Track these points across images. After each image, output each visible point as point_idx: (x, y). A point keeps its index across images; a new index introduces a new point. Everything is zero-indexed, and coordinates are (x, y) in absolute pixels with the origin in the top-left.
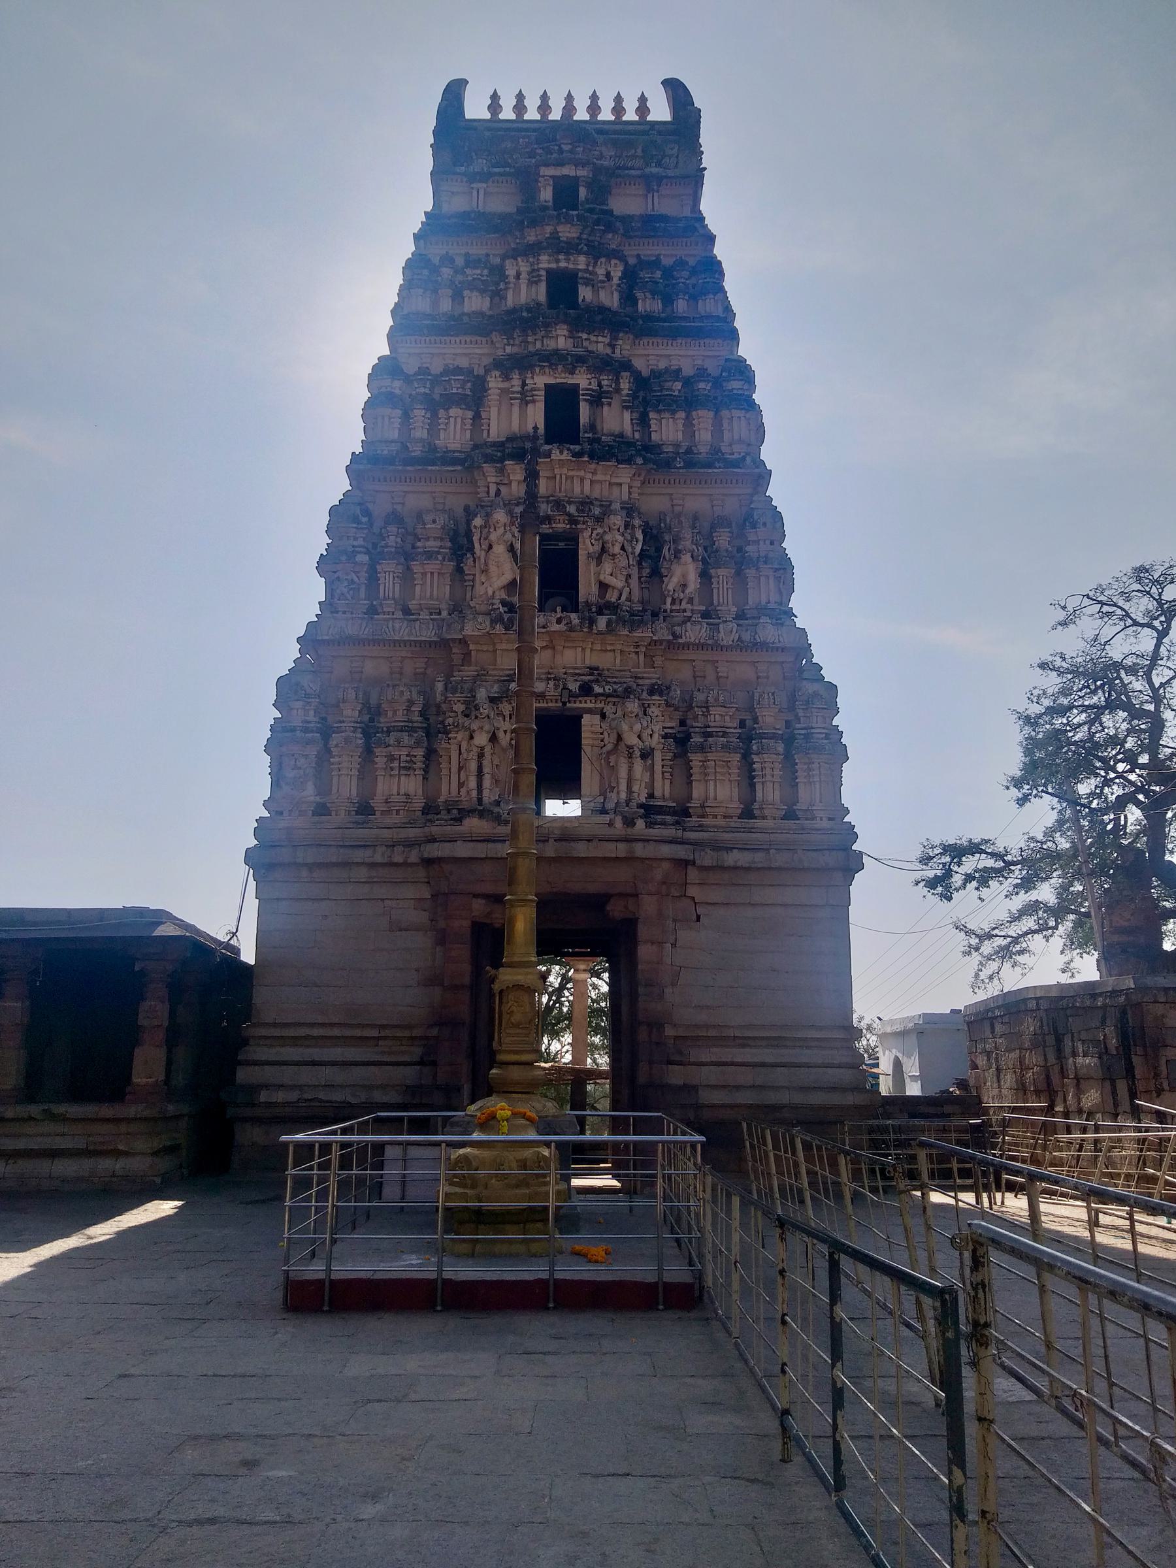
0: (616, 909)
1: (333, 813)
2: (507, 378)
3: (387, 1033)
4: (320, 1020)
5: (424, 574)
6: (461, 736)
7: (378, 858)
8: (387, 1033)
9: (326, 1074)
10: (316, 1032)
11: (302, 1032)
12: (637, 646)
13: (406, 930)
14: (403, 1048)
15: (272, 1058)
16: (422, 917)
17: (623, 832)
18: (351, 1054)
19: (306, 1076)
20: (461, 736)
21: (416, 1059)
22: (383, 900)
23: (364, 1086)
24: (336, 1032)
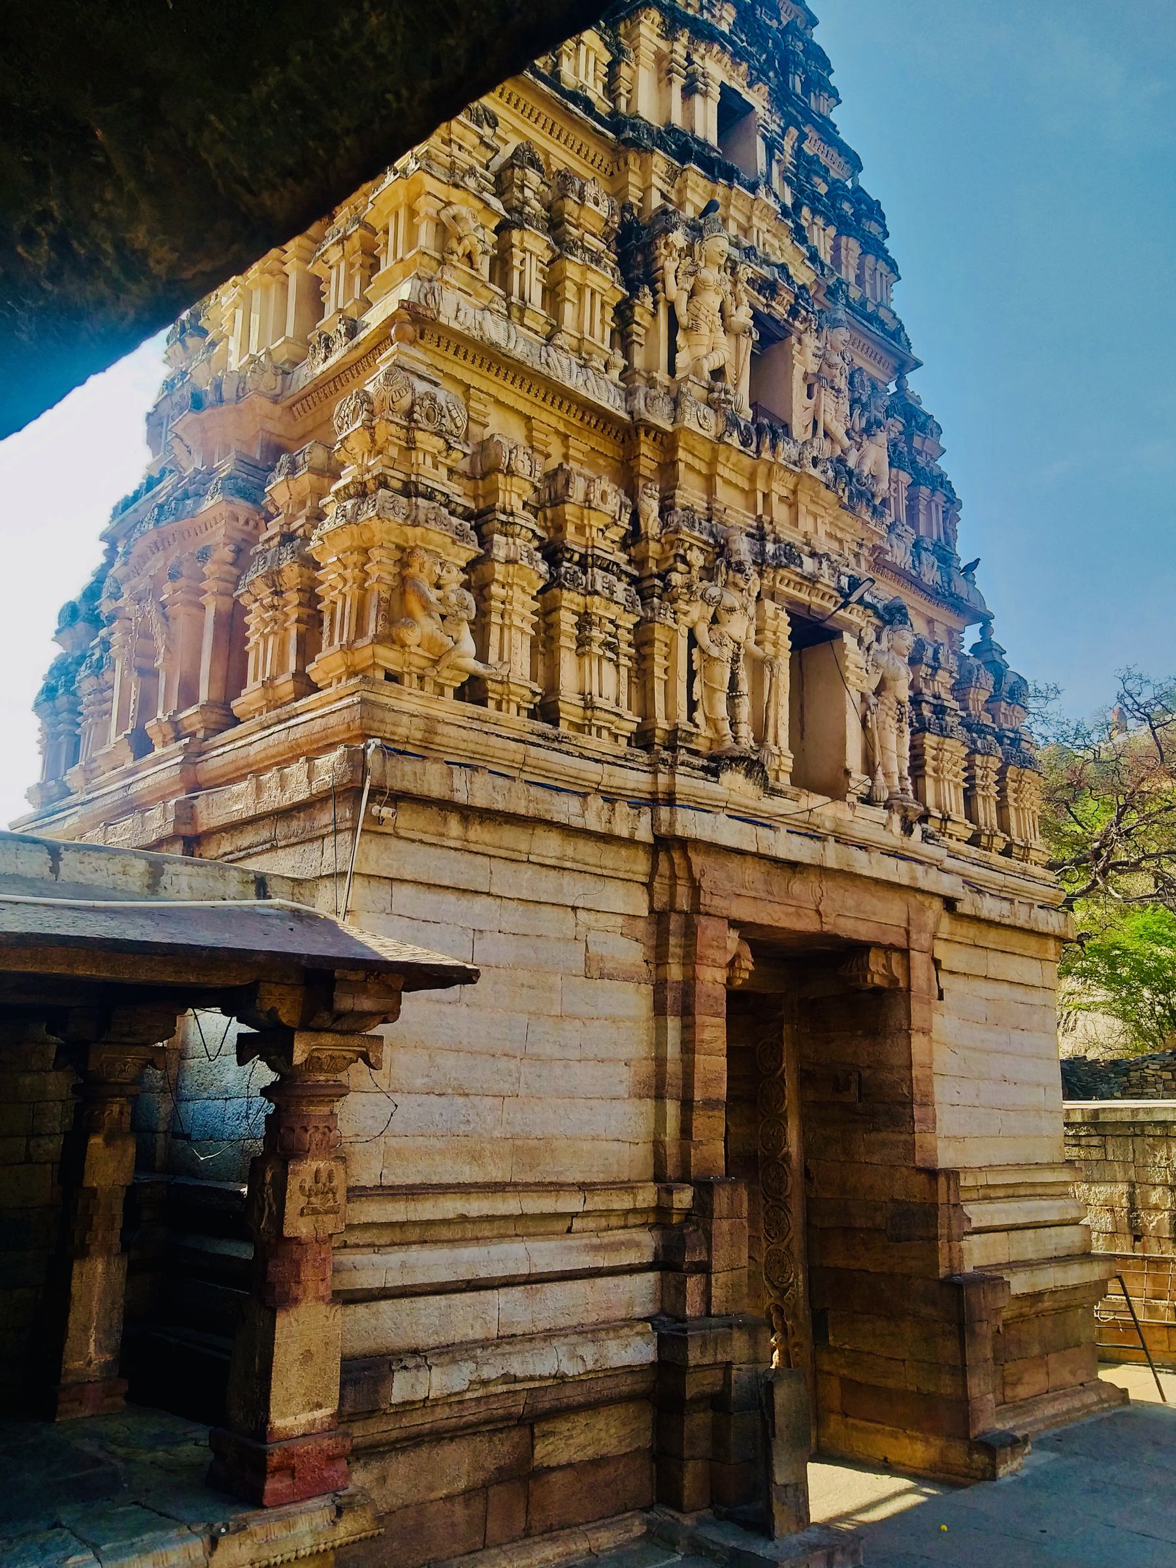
0: (877, 969)
1: (491, 703)
2: (669, 33)
3: (598, 1202)
4: (469, 1174)
5: (580, 288)
6: (697, 612)
7: (594, 823)
8: (598, 1202)
9: (508, 1309)
10: (477, 1206)
11: (450, 1207)
12: (861, 546)
13: (611, 977)
14: (621, 1235)
15: (395, 1280)
16: (631, 953)
17: (898, 843)
18: (546, 1254)
19: (466, 1318)
20: (697, 612)
21: (648, 1257)
22: (574, 908)
23: (580, 1330)
24: (509, 1205)
